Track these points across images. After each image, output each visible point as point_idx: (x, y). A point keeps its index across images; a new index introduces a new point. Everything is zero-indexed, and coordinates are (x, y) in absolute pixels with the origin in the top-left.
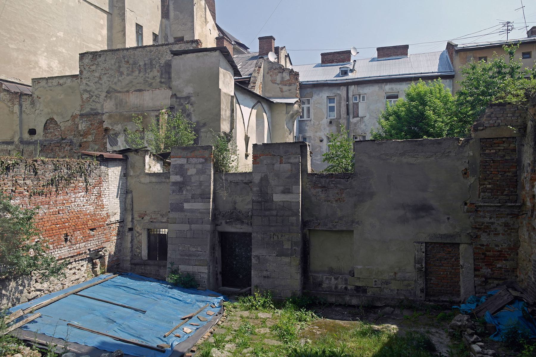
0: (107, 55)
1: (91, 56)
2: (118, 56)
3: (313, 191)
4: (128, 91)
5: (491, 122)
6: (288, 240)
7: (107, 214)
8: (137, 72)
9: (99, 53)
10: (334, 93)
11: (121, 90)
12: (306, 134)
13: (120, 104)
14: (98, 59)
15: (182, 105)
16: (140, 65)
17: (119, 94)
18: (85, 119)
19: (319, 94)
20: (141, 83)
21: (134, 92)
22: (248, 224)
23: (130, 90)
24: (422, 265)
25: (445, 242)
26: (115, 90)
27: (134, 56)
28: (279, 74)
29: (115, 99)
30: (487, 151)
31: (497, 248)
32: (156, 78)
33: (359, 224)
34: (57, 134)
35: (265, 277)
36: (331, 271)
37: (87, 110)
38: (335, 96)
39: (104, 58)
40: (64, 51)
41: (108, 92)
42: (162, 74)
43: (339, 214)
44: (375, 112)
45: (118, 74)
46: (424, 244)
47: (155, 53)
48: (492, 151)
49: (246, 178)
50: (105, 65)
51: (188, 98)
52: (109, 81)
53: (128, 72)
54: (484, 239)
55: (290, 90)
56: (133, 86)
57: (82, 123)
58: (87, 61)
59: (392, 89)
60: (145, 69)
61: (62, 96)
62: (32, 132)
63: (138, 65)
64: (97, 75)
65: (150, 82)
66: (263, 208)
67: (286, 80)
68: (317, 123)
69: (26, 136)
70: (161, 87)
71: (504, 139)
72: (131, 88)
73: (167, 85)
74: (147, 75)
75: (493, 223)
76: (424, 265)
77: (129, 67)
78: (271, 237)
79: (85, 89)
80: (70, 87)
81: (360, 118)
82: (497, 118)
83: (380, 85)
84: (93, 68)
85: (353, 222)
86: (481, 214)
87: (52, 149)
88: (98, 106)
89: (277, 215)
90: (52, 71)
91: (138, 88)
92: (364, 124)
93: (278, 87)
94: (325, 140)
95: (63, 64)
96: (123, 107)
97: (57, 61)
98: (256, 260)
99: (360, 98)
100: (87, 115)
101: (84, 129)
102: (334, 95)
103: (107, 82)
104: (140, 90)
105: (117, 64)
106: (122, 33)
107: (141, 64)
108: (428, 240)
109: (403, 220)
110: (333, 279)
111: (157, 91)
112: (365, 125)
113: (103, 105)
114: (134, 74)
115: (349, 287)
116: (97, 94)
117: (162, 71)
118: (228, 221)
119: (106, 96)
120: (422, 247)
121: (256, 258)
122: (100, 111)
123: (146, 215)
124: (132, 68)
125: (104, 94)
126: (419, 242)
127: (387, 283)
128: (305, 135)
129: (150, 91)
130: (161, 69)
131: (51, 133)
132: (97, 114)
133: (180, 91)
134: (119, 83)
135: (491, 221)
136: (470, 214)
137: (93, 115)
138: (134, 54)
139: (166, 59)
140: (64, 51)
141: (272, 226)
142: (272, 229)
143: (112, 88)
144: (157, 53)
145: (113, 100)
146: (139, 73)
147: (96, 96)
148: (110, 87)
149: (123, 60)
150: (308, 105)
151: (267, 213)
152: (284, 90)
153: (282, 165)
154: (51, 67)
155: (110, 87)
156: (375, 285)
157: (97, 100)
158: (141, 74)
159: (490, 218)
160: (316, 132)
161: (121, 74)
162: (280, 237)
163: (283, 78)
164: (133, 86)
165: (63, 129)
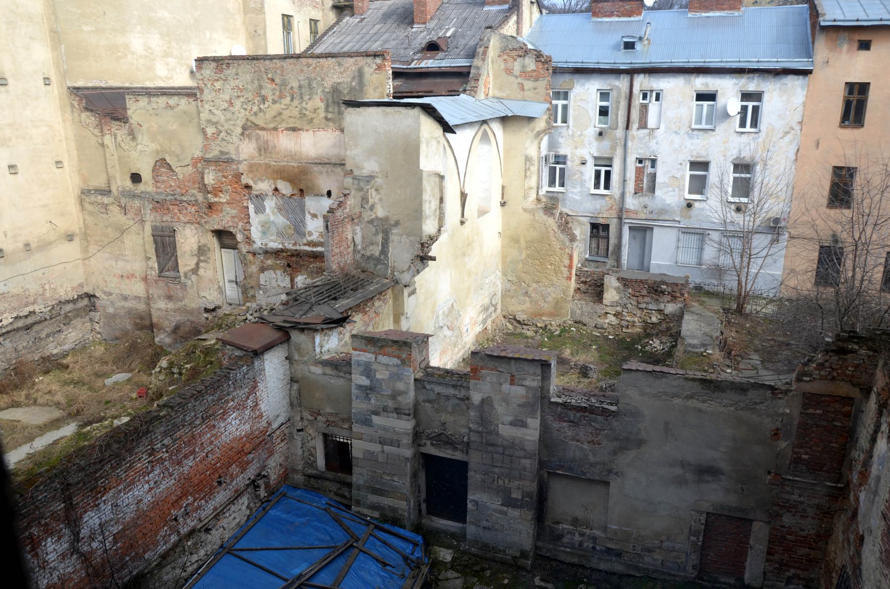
0: (239, 65)
1: (213, 65)
2: (257, 69)
3: (556, 425)
4: (275, 129)
5: (823, 373)
6: (519, 488)
7: (267, 422)
8: (289, 98)
9: (227, 61)
10: (609, 85)
11: (265, 126)
12: (559, 150)
13: (264, 149)
14: (225, 71)
15: (361, 189)
16: (292, 88)
17: (261, 133)
18: (213, 168)
19: (584, 85)
20: (295, 118)
21: (285, 132)
22: (462, 451)
23: (279, 127)
24: (698, 539)
25: (734, 515)
26: (256, 125)
27: (282, 71)
28: (519, 60)
29: (257, 140)
30: (811, 411)
31: (801, 533)
32: (318, 111)
33: (618, 476)
34: (173, 184)
35: (485, 528)
36: (575, 522)
37: (213, 153)
38: (611, 90)
40: (166, 14)
41: (244, 128)
42: (327, 106)
43: (592, 459)
44: (675, 123)
45: (258, 98)
46: (705, 515)
47: (315, 68)
48: (818, 412)
49: (460, 392)
51: (370, 178)
52: (245, 109)
53: (273, 97)
54: (787, 520)
55: (535, 89)
56: (283, 120)
57: (209, 173)
58: (208, 72)
59: (707, 85)
60: (301, 94)
61: (175, 126)
63: (289, 86)
64: (227, 98)
65: (309, 117)
66: (484, 440)
67: (529, 70)
68: (579, 133)
69: (128, 183)
70: (327, 126)
71: (836, 398)
72: (280, 123)
73: (336, 125)
74: (304, 105)
75: (802, 503)
76: (701, 539)
77: (276, 89)
78: (494, 481)
79: (208, 118)
80: (185, 113)
81: (648, 131)
82: (833, 369)
83: (687, 76)
84: (218, 85)
85: (610, 471)
86: (788, 489)
87: (168, 209)
88: (231, 149)
89: (503, 454)
90: (152, 54)
91: (292, 126)
92: (655, 141)
93: (516, 81)
94: (591, 163)
95: (167, 39)
96: (270, 153)
97: (158, 36)
98: (473, 505)
99: (651, 96)
100: (216, 162)
101: (212, 182)
102: (609, 88)
103: (242, 110)
104: (294, 129)
107: (294, 85)
108: (711, 510)
109: (681, 482)
110: (577, 535)
112: (657, 143)
113: (238, 148)
115: (598, 548)
116: (228, 129)
117: (327, 100)
118: (435, 442)
119: (242, 134)
120: (701, 518)
121: (473, 503)
122: (234, 157)
123: (320, 415)
124: (281, 91)
126: (698, 512)
127: (649, 550)
128: (558, 152)
129: (311, 132)
130: (325, 96)
131: (164, 181)
132: (229, 161)
133: (358, 167)
134: (262, 114)
135: (799, 499)
136: (773, 487)
137: (223, 162)
138: (282, 67)
139: (333, 81)
140: (166, 14)
141: (496, 466)
142: (497, 470)
143: (251, 121)
144: (318, 69)
147: (226, 132)
148: (247, 120)
149: (265, 77)
150: (565, 102)
151: (489, 448)
152: (526, 88)
153: (514, 388)
154: (150, 48)
155: (247, 120)
156: (634, 550)
159: (800, 496)
160: (576, 148)
161: (264, 99)
162: (506, 481)
163: (524, 66)
164: (283, 120)
165: (181, 177)
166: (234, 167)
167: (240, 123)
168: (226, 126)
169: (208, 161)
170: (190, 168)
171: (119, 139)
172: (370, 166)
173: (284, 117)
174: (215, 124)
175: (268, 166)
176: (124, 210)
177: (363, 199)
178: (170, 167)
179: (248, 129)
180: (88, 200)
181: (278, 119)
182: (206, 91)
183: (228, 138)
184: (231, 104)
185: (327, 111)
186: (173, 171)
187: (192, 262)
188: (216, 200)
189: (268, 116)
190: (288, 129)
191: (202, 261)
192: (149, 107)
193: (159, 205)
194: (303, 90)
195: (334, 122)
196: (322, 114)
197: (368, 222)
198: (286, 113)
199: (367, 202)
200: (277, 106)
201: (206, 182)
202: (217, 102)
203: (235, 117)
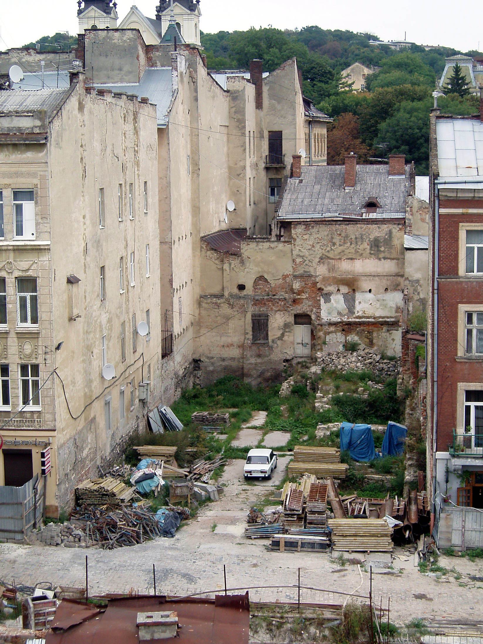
1: (303, 227)
4: (340, 259)
13: (332, 269)
15: (413, 286)
16: (351, 239)
26: (328, 257)
27: (346, 231)
37: (300, 271)
39: (317, 230)
41: (321, 258)
42: (371, 247)
50: (318, 236)
51: (418, 281)
57: (296, 283)
58: (300, 230)
61: (273, 258)
62: (241, 287)
64: (311, 243)
69: (236, 291)
70: (371, 257)
72: (343, 256)
74: (358, 247)
80: (281, 251)
84: (306, 237)
87: (265, 304)
88: (311, 270)
100: (301, 276)
101: (298, 287)
104: (352, 259)
105: (330, 236)
106: (243, 148)
111: (367, 261)
113: (315, 269)
114: (346, 245)
119: (319, 262)
122: (313, 274)
124: (344, 240)
125: (318, 260)
129: (361, 260)
131: (260, 288)
132: (310, 276)
133: (411, 277)
134: (332, 251)
137: (305, 277)
138: (346, 228)
144: (367, 230)
145: (326, 265)
146: (351, 244)
148: (323, 254)
149: (336, 233)
155: (323, 254)
157: (310, 264)
158: (353, 246)
161: (334, 244)
165: (273, 285)
166: (314, 279)
167: (319, 256)
168: (309, 258)
169: (295, 277)
170: (281, 280)
171: (232, 266)
172: (417, 276)
173: (345, 253)
174: (302, 257)
175: (334, 278)
176: (232, 306)
177: (414, 290)
178: (266, 280)
179: (323, 259)
180: (205, 301)
181: (342, 254)
182: (298, 240)
183: (310, 264)
184: (313, 246)
185: (371, 249)
186: (268, 282)
187: (279, 333)
188: (299, 297)
189: (336, 252)
190: (346, 259)
191: (287, 332)
192: (257, 248)
193: (257, 302)
194: (358, 240)
195: (375, 255)
196: (368, 251)
197: (417, 300)
198: (347, 251)
199: (416, 291)
200: (342, 248)
201: (294, 287)
202: (304, 245)
203: (315, 253)
